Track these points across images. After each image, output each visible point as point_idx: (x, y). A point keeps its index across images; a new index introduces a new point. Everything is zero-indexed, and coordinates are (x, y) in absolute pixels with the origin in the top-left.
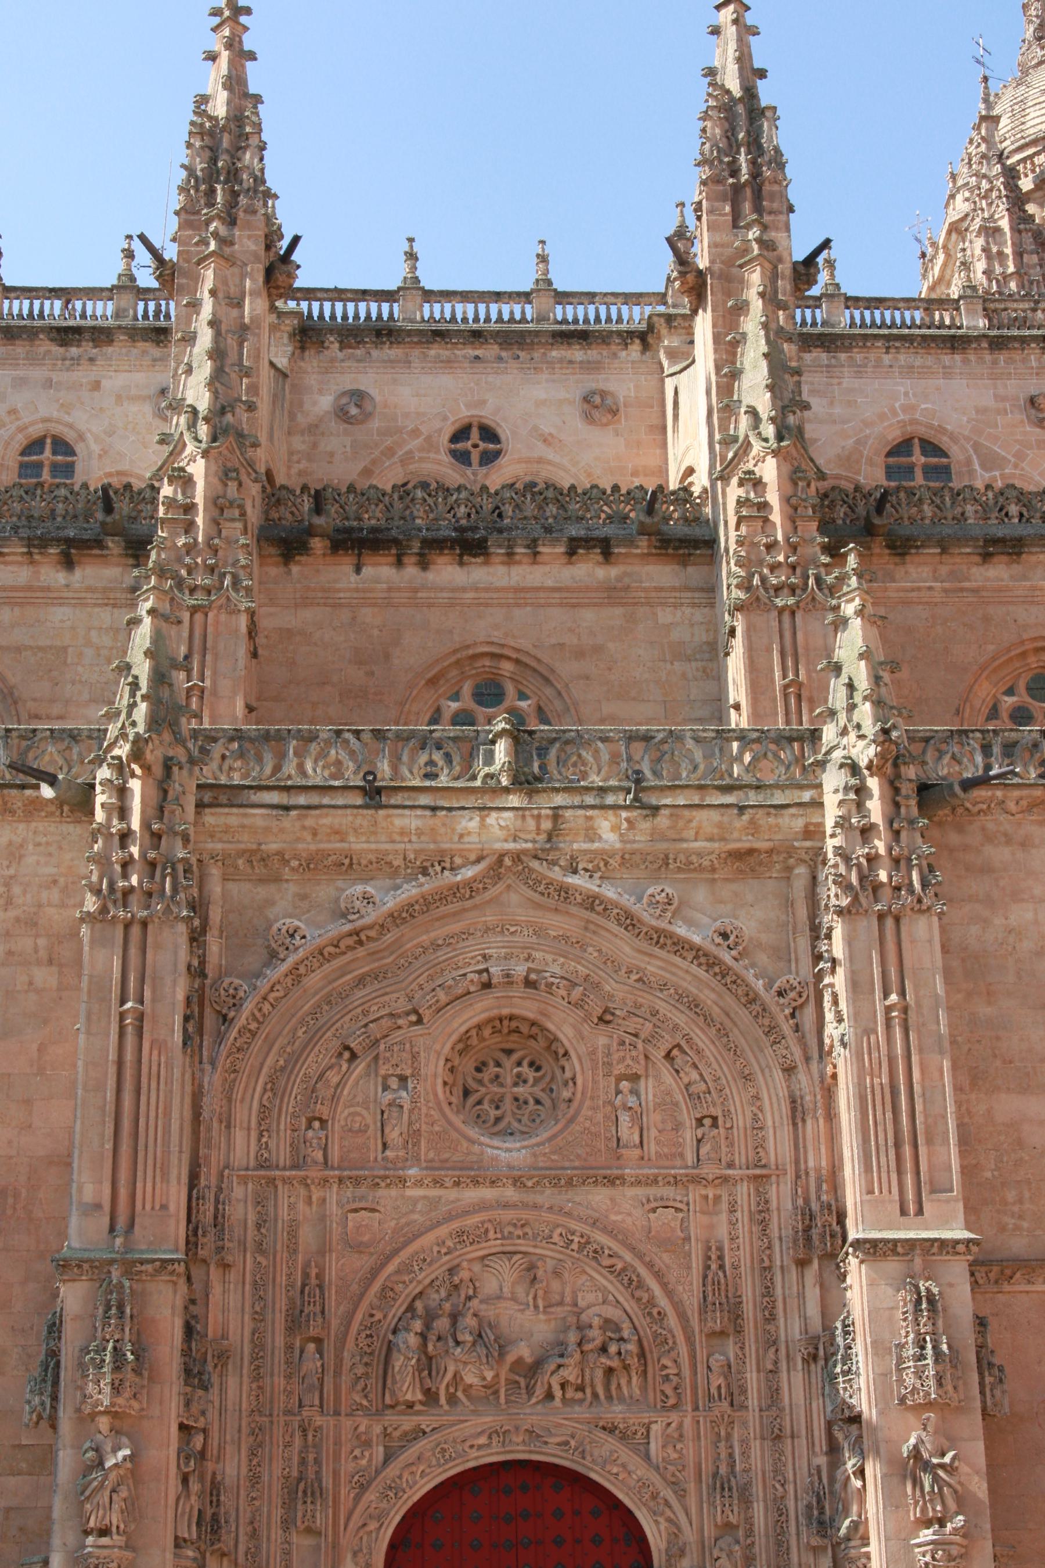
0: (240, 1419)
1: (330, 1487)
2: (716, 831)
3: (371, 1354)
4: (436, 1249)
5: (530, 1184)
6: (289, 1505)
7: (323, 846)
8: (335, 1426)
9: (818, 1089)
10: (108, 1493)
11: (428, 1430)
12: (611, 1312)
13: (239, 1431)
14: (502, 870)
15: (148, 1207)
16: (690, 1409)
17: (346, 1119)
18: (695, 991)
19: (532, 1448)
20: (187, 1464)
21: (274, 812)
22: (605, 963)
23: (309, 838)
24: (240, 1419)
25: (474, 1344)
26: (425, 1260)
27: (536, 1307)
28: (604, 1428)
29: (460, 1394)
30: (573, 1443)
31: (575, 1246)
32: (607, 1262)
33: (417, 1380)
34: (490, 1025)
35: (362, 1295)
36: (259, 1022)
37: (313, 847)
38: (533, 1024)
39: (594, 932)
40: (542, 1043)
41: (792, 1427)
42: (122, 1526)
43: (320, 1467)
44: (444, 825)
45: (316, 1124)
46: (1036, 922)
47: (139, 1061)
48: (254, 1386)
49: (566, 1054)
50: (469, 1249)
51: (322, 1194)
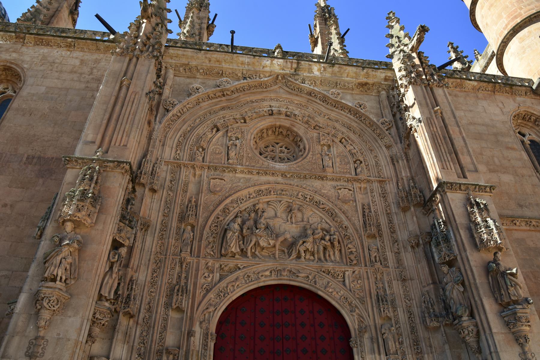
0: (150, 255)
1: (192, 289)
2: (354, 75)
3: (216, 234)
4: (248, 196)
5: (288, 176)
6: (170, 296)
7: (212, 65)
8: (197, 262)
9: (402, 151)
10: (59, 258)
11: (241, 267)
12: (325, 226)
13: (149, 260)
14: (278, 81)
15: (117, 144)
16: (363, 265)
17: (213, 149)
18: (350, 123)
19: (291, 278)
20: (114, 258)
21: (196, 51)
22: (315, 113)
23: (208, 62)
24: (150, 255)
25: (265, 230)
26: (243, 199)
27: (292, 223)
28: (324, 272)
29: (257, 253)
30: (310, 277)
31: (308, 200)
32: (322, 206)
33: (237, 243)
34: (271, 130)
35: (214, 210)
36: (181, 113)
37: (209, 65)
38: (288, 129)
39: (311, 103)
40: (291, 139)
41: (410, 276)
42: (64, 278)
43: (187, 280)
44: (258, 61)
45: (201, 150)
46: (465, 116)
47: (125, 98)
48: (160, 242)
49: (301, 140)
50: (262, 197)
51: (200, 172)
